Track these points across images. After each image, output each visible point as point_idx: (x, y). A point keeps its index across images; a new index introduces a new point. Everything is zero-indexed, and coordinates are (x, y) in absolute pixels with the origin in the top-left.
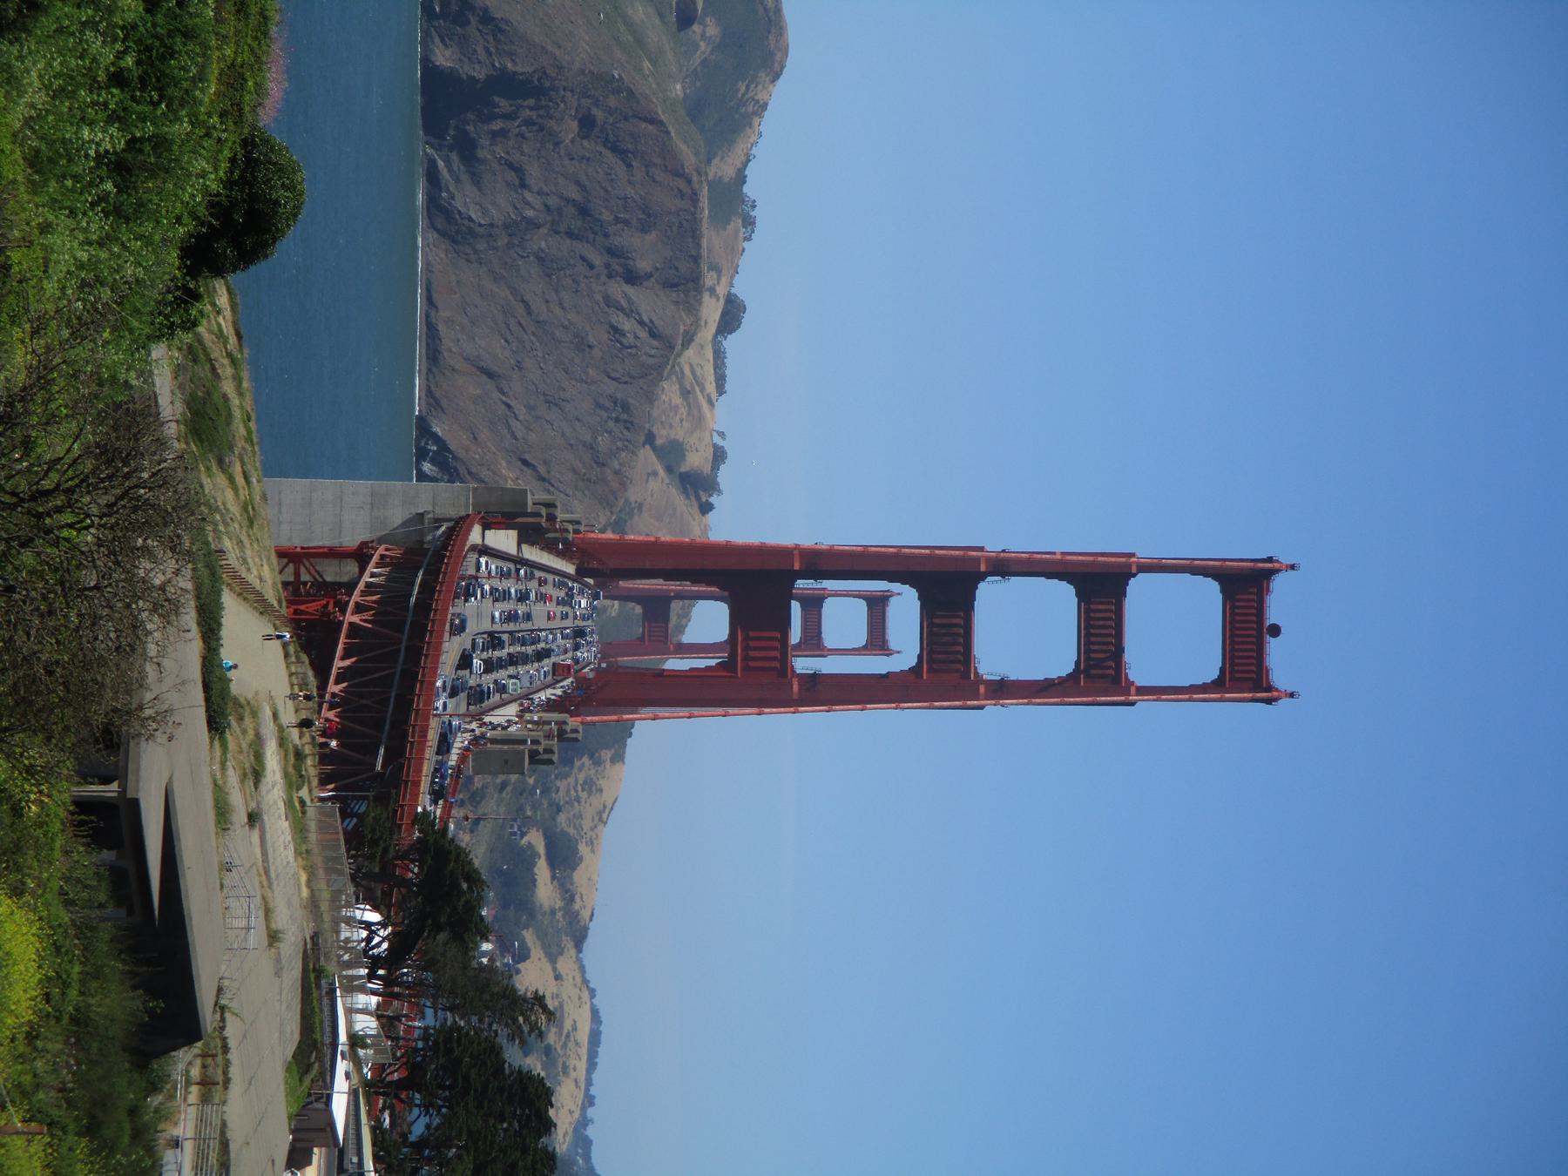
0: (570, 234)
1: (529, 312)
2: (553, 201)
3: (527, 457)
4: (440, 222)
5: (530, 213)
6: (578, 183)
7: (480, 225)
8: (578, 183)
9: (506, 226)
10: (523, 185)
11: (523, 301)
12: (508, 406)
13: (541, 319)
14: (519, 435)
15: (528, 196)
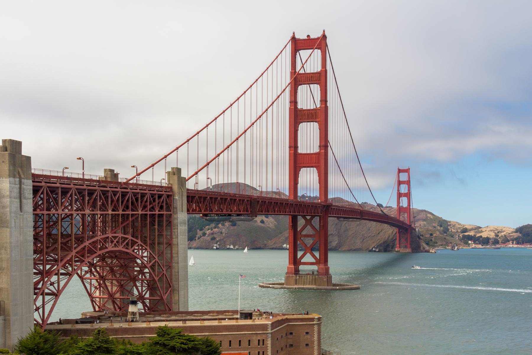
0: (341, 227)
1: (354, 233)
2: (335, 229)
3: (378, 233)
4: (337, 248)
5: (337, 233)
6: (332, 225)
7: (338, 241)
8: (332, 225)
9: (339, 237)
10: (332, 234)
11: (352, 234)
12: (369, 237)
13: (355, 231)
14: (374, 235)
15: (334, 233)
